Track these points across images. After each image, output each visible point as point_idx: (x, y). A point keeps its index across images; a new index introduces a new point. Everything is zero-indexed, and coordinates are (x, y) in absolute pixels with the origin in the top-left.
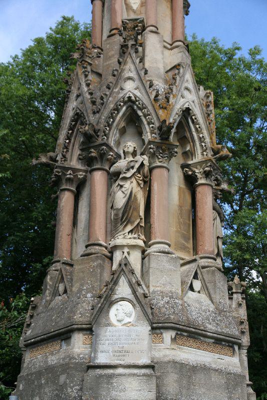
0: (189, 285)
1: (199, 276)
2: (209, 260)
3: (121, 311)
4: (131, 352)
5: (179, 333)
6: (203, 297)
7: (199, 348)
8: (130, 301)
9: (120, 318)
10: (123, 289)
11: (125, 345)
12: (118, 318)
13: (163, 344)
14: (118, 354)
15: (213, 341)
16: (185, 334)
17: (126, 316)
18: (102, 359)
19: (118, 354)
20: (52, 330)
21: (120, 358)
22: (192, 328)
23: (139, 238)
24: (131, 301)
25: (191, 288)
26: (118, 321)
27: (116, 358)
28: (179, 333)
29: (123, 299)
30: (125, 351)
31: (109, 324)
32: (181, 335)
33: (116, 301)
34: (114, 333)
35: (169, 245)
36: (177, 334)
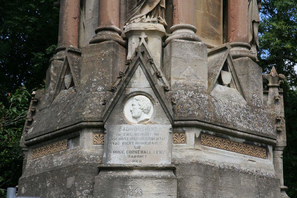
0: (217, 77)
1: (230, 67)
2: (242, 49)
3: (137, 107)
4: (148, 152)
5: (204, 132)
6: (234, 91)
7: (227, 149)
8: (147, 95)
9: (136, 114)
10: (140, 81)
11: (142, 145)
12: (134, 115)
13: (185, 144)
14: (134, 155)
15: (244, 141)
16: (212, 133)
17: (143, 113)
18: (115, 160)
19: (134, 155)
20: (58, 128)
21: (137, 159)
22: (219, 126)
23: (159, 22)
24: (149, 95)
25: (220, 81)
26: (135, 118)
27: (132, 159)
28: (204, 132)
29: (140, 93)
30: (142, 152)
31: (124, 122)
32: (207, 134)
33: (130, 95)
34: (130, 132)
35: (195, 31)
36: (202, 133)
